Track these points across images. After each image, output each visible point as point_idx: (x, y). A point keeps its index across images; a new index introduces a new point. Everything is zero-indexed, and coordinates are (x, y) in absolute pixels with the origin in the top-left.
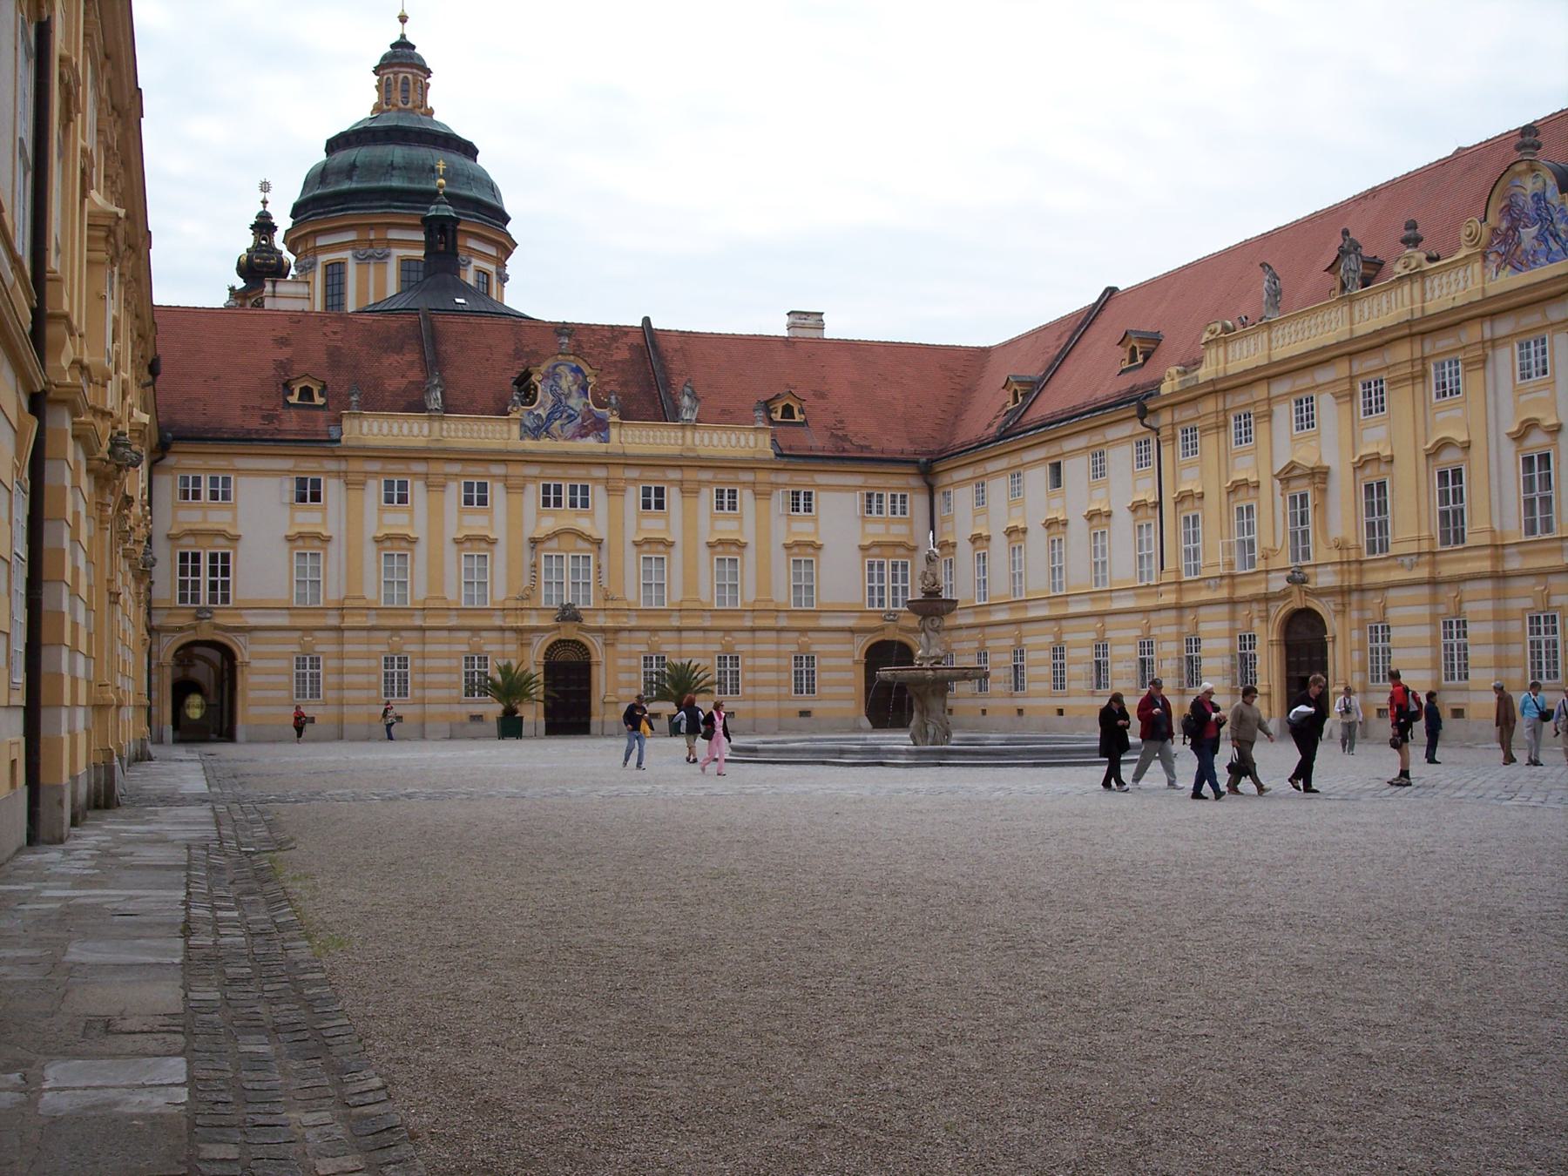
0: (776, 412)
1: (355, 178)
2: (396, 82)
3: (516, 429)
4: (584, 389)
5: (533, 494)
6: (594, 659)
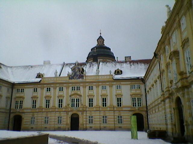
5: (70, 88)
6: (79, 117)
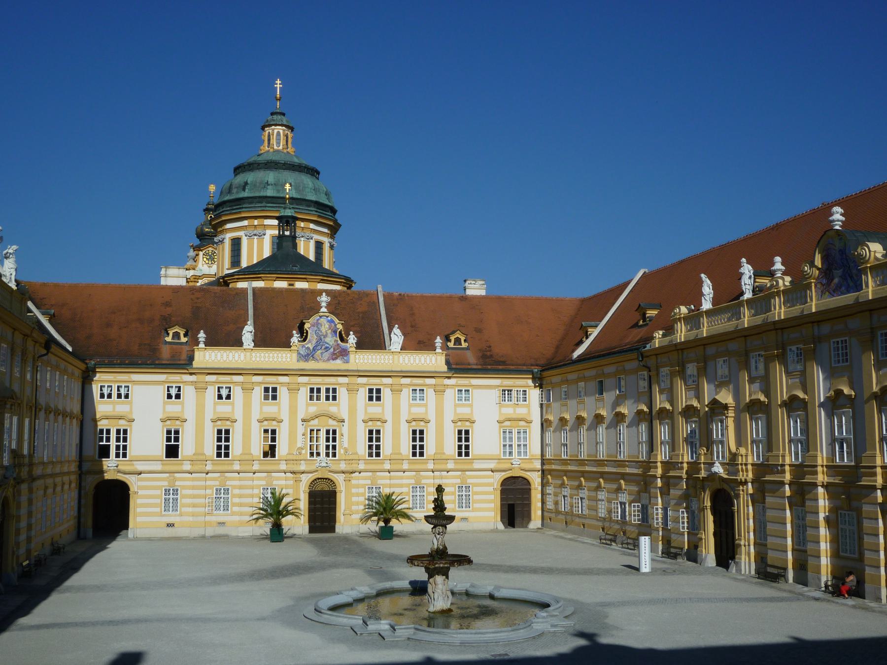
0: (450, 342)
1: (247, 190)
2: (273, 135)
3: (295, 355)
4: (335, 332)
5: (304, 393)
